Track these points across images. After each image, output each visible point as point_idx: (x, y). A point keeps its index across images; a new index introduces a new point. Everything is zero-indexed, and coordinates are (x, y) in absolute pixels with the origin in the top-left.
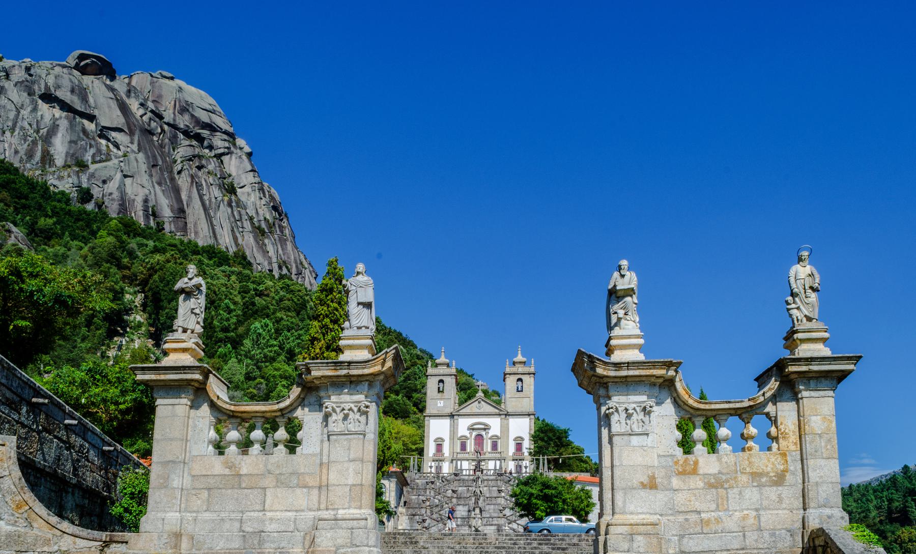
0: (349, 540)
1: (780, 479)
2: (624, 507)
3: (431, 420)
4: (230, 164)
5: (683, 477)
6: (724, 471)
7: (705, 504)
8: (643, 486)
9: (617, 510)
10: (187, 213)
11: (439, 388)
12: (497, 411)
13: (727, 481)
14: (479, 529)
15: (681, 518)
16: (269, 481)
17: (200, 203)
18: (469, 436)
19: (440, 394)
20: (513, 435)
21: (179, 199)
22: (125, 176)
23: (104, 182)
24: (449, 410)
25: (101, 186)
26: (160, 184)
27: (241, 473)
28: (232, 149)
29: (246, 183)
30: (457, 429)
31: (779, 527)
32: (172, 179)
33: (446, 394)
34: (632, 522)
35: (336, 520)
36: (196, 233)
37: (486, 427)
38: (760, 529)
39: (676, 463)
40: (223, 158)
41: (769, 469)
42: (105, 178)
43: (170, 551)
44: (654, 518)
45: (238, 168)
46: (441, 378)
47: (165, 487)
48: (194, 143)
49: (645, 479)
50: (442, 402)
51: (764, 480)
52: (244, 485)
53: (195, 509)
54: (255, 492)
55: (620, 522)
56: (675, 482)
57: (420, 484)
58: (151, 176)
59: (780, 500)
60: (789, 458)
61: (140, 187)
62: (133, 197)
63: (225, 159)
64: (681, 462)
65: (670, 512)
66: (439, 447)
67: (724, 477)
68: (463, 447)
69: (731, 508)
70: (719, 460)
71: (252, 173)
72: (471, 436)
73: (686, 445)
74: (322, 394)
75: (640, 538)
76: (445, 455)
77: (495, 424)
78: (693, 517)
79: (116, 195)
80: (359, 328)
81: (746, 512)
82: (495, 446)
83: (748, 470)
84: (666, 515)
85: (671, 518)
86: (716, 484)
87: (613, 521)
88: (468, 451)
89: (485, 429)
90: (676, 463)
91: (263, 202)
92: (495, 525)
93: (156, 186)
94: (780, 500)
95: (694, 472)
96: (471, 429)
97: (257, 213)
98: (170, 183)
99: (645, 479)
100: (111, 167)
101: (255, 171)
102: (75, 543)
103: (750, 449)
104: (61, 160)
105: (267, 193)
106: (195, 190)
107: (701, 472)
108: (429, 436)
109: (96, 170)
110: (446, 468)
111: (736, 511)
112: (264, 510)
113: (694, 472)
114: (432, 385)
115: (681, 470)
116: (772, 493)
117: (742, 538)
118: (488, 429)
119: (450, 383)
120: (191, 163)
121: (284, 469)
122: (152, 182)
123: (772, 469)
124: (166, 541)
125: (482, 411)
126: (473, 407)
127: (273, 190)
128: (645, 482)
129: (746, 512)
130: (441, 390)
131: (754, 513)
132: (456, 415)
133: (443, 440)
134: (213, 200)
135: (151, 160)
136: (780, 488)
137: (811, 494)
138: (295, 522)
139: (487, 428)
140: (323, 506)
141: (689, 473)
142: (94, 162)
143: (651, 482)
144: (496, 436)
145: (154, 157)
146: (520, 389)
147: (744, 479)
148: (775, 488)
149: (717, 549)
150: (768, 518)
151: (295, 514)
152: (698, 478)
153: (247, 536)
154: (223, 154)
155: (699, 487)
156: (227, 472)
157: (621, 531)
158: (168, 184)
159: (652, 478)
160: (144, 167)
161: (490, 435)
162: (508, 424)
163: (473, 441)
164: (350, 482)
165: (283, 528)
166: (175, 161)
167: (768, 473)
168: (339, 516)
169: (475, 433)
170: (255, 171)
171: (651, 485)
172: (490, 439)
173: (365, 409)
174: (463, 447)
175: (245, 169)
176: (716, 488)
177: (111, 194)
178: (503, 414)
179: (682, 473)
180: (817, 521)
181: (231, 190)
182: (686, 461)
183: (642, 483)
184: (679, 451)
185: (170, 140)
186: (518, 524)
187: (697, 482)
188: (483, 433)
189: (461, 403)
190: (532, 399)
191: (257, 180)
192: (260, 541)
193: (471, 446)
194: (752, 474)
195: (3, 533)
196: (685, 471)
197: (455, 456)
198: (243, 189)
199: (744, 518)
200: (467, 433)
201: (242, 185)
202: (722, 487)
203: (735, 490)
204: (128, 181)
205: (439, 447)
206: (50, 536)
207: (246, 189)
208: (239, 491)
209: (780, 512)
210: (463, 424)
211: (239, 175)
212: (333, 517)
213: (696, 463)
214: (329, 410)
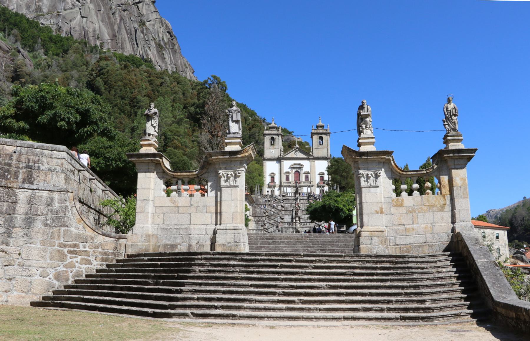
0: (233, 239)
1: (442, 208)
2: (368, 223)
4: (142, 8)
5: (396, 208)
6: (416, 205)
7: (406, 220)
8: (377, 212)
9: (365, 224)
10: (118, 37)
11: (271, 142)
13: (417, 209)
15: (396, 228)
16: (192, 210)
17: (125, 31)
18: (290, 172)
19: (272, 146)
20: (318, 171)
21: (113, 29)
22: (83, 17)
23: (71, 21)
24: (277, 156)
25: (69, 23)
26: (102, 21)
27: (179, 205)
29: (152, 19)
30: (283, 167)
31: (442, 232)
32: (109, 18)
33: (276, 146)
34: (372, 230)
35: (226, 229)
36: (123, 49)
38: (433, 233)
39: (393, 201)
41: (437, 204)
43: (147, 243)
44: (382, 229)
45: (147, 10)
47: (143, 212)
49: (378, 210)
50: (273, 151)
51: (435, 209)
52: (180, 212)
53: (157, 223)
54: (186, 215)
55: (367, 230)
56: (393, 210)
57: (262, 202)
58: (97, 16)
59: (443, 218)
60: (446, 198)
61: (91, 23)
62: (87, 29)
64: (395, 200)
65: (390, 225)
66: (273, 179)
67: (416, 208)
68: (287, 178)
69: (419, 223)
70: (413, 199)
71: (155, 13)
72: (292, 172)
73: (398, 192)
74: (217, 167)
75: (376, 238)
76: (276, 184)
77: (306, 165)
78: (402, 227)
79: (77, 28)
80: (234, 133)
81: (426, 225)
82: (307, 178)
83: (427, 204)
84: (389, 226)
85: (391, 228)
86: (412, 211)
87: (362, 230)
88: (290, 181)
90: (393, 201)
91: (161, 29)
93: (100, 22)
94: (443, 218)
95: (401, 205)
96: (292, 167)
97: (159, 36)
99: (378, 210)
100: (75, 12)
101: (157, 12)
102: (104, 239)
103: (428, 194)
104: (46, 9)
106: (123, 24)
107: (405, 205)
108: (266, 172)
109: (66, 14)
110: (277, 192)
111: (422, 224)
112: (190, 224)
113: (401, 205)
114: (267, 140)
115: (395, 204)
116: (438, 215)
117: (425, 237)
118: (302, 167)
119: (279, 141)
120: (120, 8)
121: (199, 204)
122: (98, 20)
123: (439, 203)
124: (145, 238)
126: (292, 154)
127: (167, 22)
128: (378, 211)
129: (426, 225)
130: (273, 143)
131: (430, 225)
133: (274, 174)
134: (133, 30)
136: (442, 212)
137: (457, 216)
138: (206, 230)
139: (301, 167)
140: (219, 223)
141: (399, 206)
142: (65, 10)
143: (380, 210)
144: (307, 172)
145: (99, 6)
146: (321, 143)
147: (426, 208)
148: (440, 213)
149: (413, 243)
150: (437, 228)
151: (205, 226)
152: (404, 208)
153: (183, 237)
155: (404, 212)
156: (172, 205)
157: (366, 235)
158: (107, 20)
159: (381, 208)
160: (93, 12)
162: (314, 165)
163: (293, 175)
164: (232, 211)
165: (200, 233)
166: (111, 8)
167: (437, 205)
168: (228, 228)
169: (294, 170)
170: (157, 12)
171: (382, 213)
172: (304, 174)
173: (239, 175)
174: (287, 178)
175: (151, 10)
176: (412, 213)
177: (74, 28)
179: (396, 206)
180: (460, 228)
181: (142, 23)
182: (397, 200)
183: (376, 211)
184: (394, 195)
187: (402, 210)
189: (285, 151)
190: (329, 149)
191: (158, 17)
192: (189, 239)
193: (292, 178)
194: (429, 206)
195: (73, 234)
196: (397, 205)
197: (282, 184)
198: (150, 22)
199: (426, 227)
200: (289, 170)
201: (149, 20)
202: (415, 212)
203: (422, 214)
204: (85, 19)
205: (273, 179)
206: (93, 235)
207: (152, 22)
208: (178, 214)
209: (443, 224)
210: (287, 165)
212: (225, 228)
213: (402, 200)
214: (221, 175)
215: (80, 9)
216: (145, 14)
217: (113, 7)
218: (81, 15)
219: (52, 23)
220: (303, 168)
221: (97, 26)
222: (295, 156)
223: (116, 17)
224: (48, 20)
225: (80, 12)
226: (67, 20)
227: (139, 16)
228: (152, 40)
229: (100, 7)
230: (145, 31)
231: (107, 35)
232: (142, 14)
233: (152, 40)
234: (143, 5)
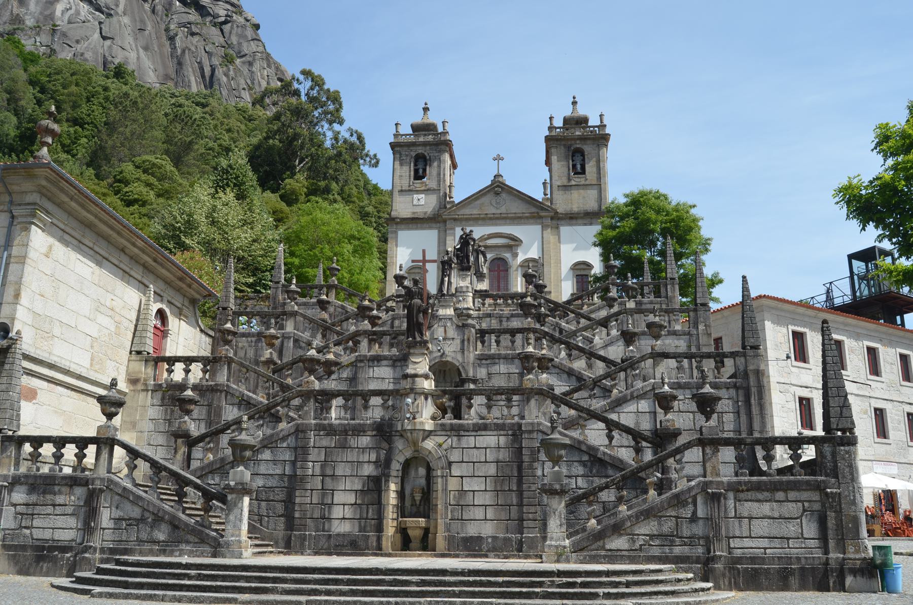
3: (400, 232)
4: (230, 33)
11: (416, 171)
12: (534, 210)
14: (429, 444)
22: (104, 38)
23: (78, 42)
26: (146, 49)
28: (234, 18)
29: (247, 52)
37: (512, 243)
40: (224, 27)
42: (79, 38)
46: (420, 150)
48: (193, 11)
58: (136, 39)
62: (110, 59)
63: (227, 28)
89: (509, 247)
92: (499, 427)
93: (141, 50)
98: (159, 49)
100: (88, 27)
105: (273, 65)
109: (70, 29)
118: (517, 246)
120: (186, 30)
122: (136, 46)
125: (503, 210)
130: (421, 171)
132: (450, 219)
135: (138, 24)
144: (534, 260)
145: (142, 21)
154: (225, 22)
158: (156, 49)
161: (521, 258)
175: (246, 36)
178: (546, 217)
185: (163, 6)
186: (612, 426)
188: (507, 255)
204: (108, 42)
211: (240, 44)
215: (100, 23)
216: (235, 43)
217: (172, 27)
218: (101, 33)
219: (38, 44)
220: (519, 251)
221: (133, 56)
222: (494, 211)
223: (175, 44)
224: (30, 38)
225: (101, 29)
226: (69, 39)
227: (224, 47)
228: (244, 89)
229: (145, 24)
230: (232, 73)
231: (151, 73)
232: (229, 43)
233: (244, 89)
234: (232, 28)
